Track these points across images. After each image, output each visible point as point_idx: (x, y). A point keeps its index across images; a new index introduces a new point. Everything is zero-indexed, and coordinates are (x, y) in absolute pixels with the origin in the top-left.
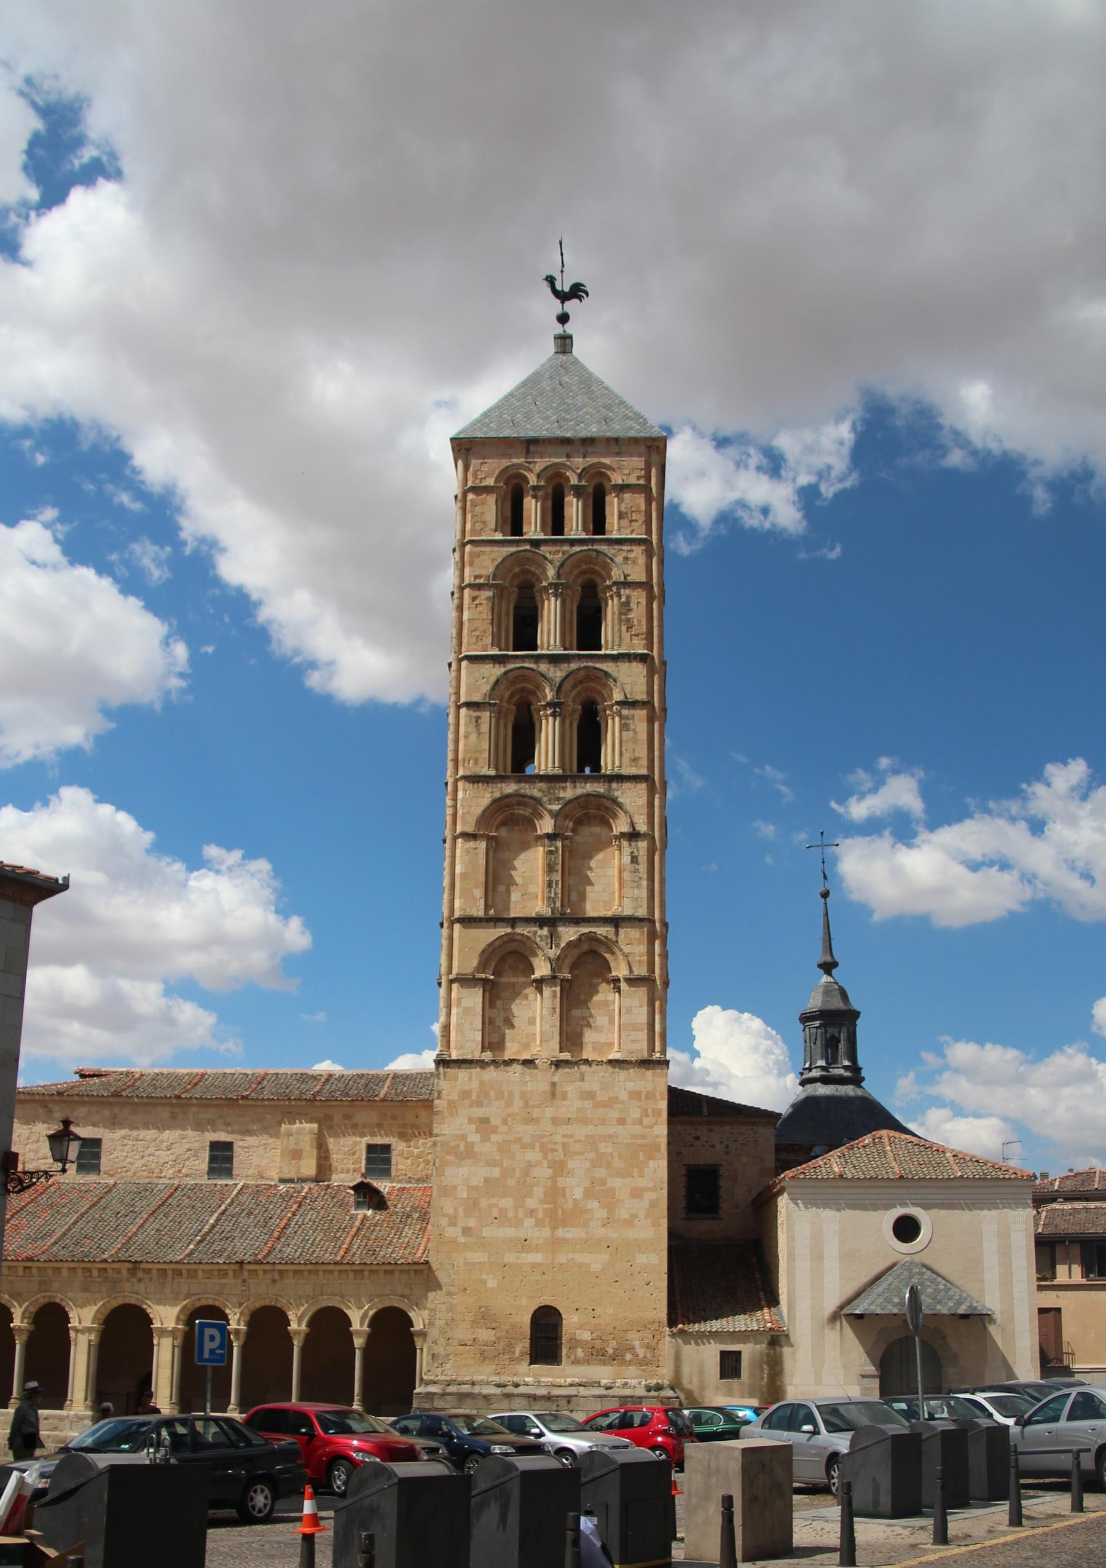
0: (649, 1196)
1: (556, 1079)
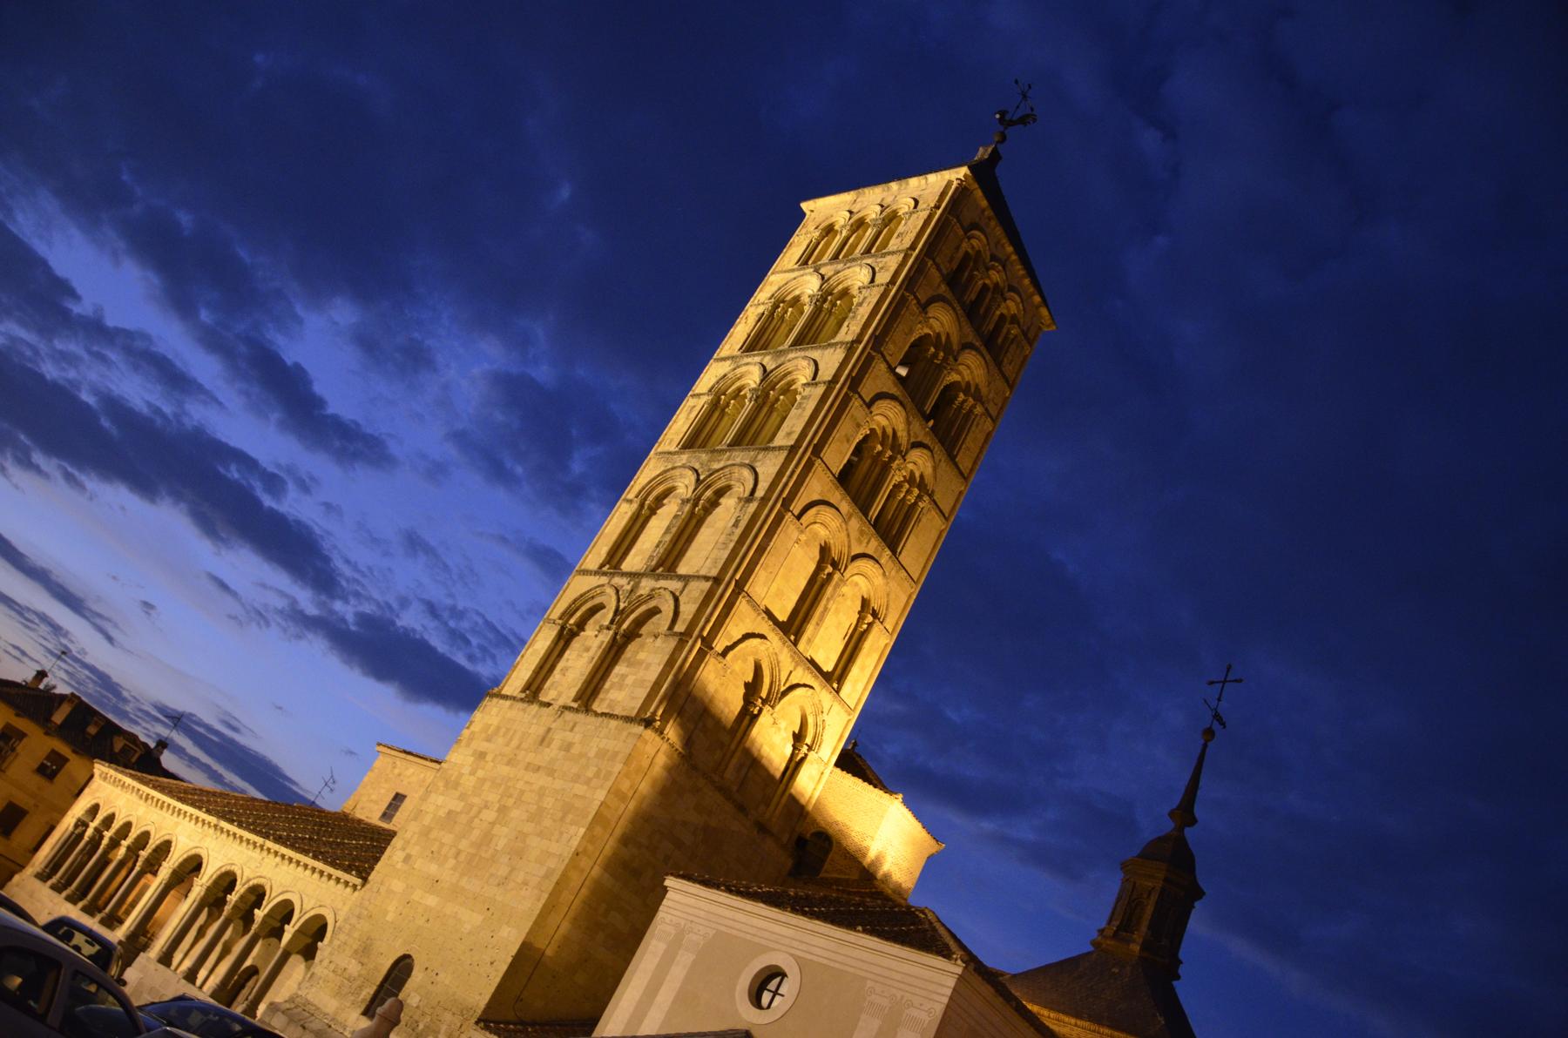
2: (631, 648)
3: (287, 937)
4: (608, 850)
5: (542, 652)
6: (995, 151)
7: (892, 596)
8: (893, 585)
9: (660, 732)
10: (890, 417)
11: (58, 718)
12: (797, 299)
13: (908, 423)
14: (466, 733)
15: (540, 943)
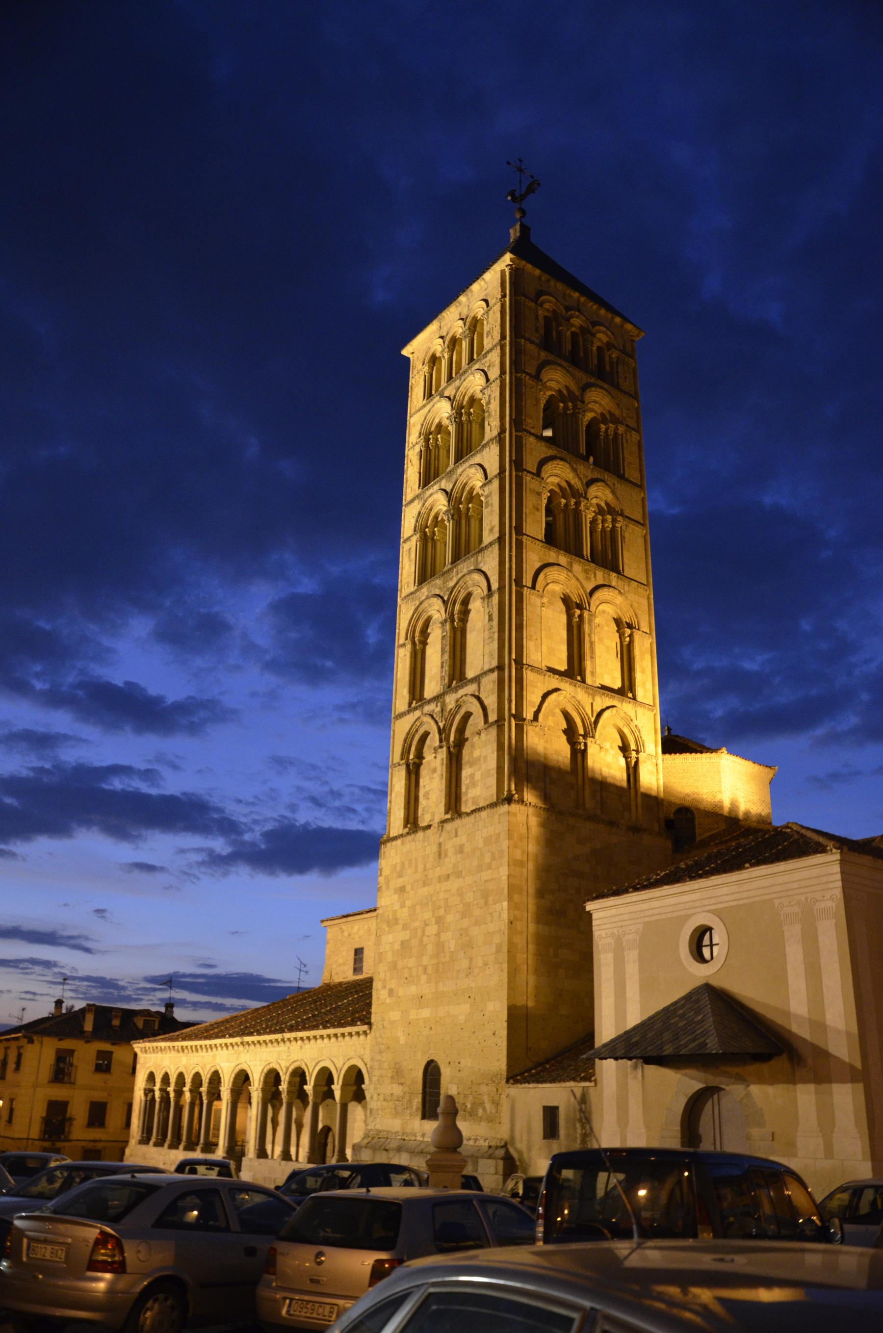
0: (497, 940)
1: (441, 840)
2: (465, 752)
3: (337, 1094)
4: (532, 908)
5: (403, 791)
6: (522, 226)
7: (635, 605)
8: (632, 597)
9: (521, 801)
10: (558, 474)
11: (88, 1026)
12: (440, 426)
13: (574, 470)
14: (381, 880)
15: (521, 1001)
